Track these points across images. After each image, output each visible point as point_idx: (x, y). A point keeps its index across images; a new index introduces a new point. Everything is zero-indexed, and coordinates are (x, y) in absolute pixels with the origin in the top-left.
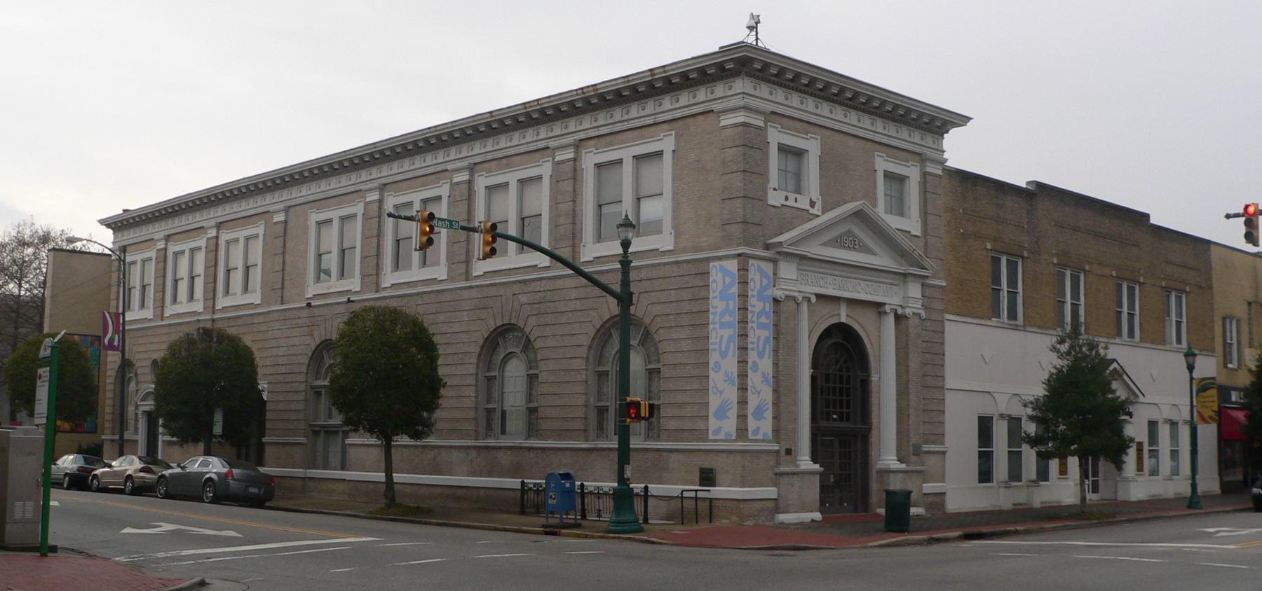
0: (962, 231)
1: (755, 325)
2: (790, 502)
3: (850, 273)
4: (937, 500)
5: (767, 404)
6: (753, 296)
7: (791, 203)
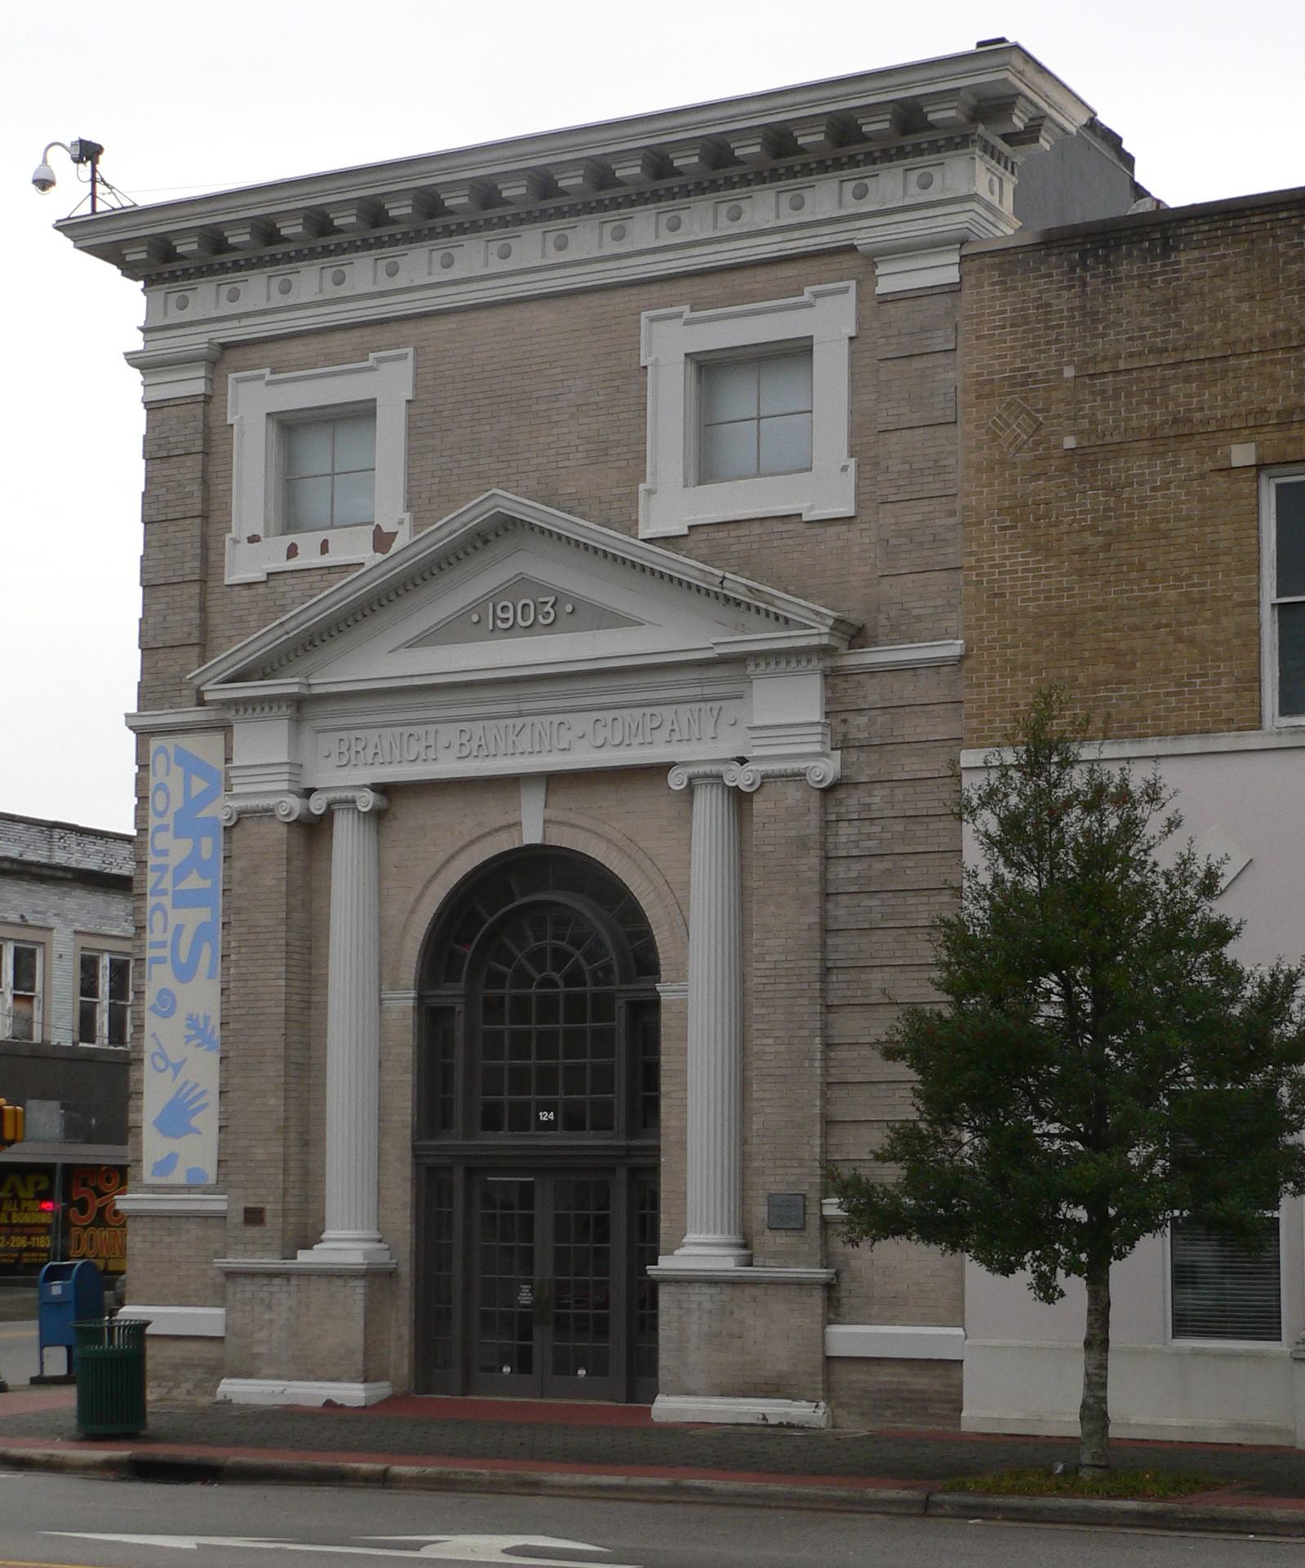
0: (1070, 442)
1: (167, 901)
2: (258, 1349)
3: (518, 700)
4: (923, 1382)
5: (204, 1093)
6: (165, 828)
7: (310, 557)
